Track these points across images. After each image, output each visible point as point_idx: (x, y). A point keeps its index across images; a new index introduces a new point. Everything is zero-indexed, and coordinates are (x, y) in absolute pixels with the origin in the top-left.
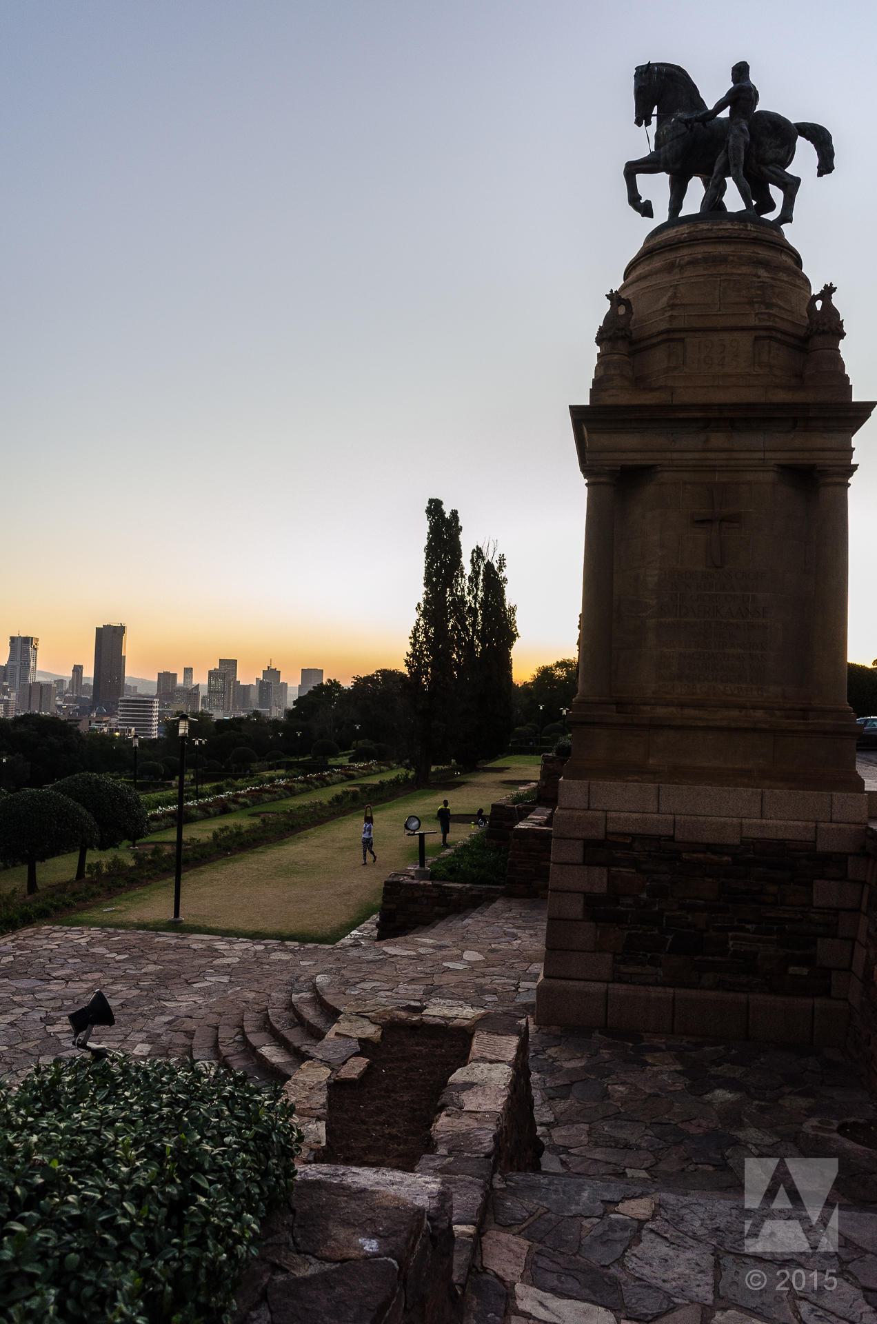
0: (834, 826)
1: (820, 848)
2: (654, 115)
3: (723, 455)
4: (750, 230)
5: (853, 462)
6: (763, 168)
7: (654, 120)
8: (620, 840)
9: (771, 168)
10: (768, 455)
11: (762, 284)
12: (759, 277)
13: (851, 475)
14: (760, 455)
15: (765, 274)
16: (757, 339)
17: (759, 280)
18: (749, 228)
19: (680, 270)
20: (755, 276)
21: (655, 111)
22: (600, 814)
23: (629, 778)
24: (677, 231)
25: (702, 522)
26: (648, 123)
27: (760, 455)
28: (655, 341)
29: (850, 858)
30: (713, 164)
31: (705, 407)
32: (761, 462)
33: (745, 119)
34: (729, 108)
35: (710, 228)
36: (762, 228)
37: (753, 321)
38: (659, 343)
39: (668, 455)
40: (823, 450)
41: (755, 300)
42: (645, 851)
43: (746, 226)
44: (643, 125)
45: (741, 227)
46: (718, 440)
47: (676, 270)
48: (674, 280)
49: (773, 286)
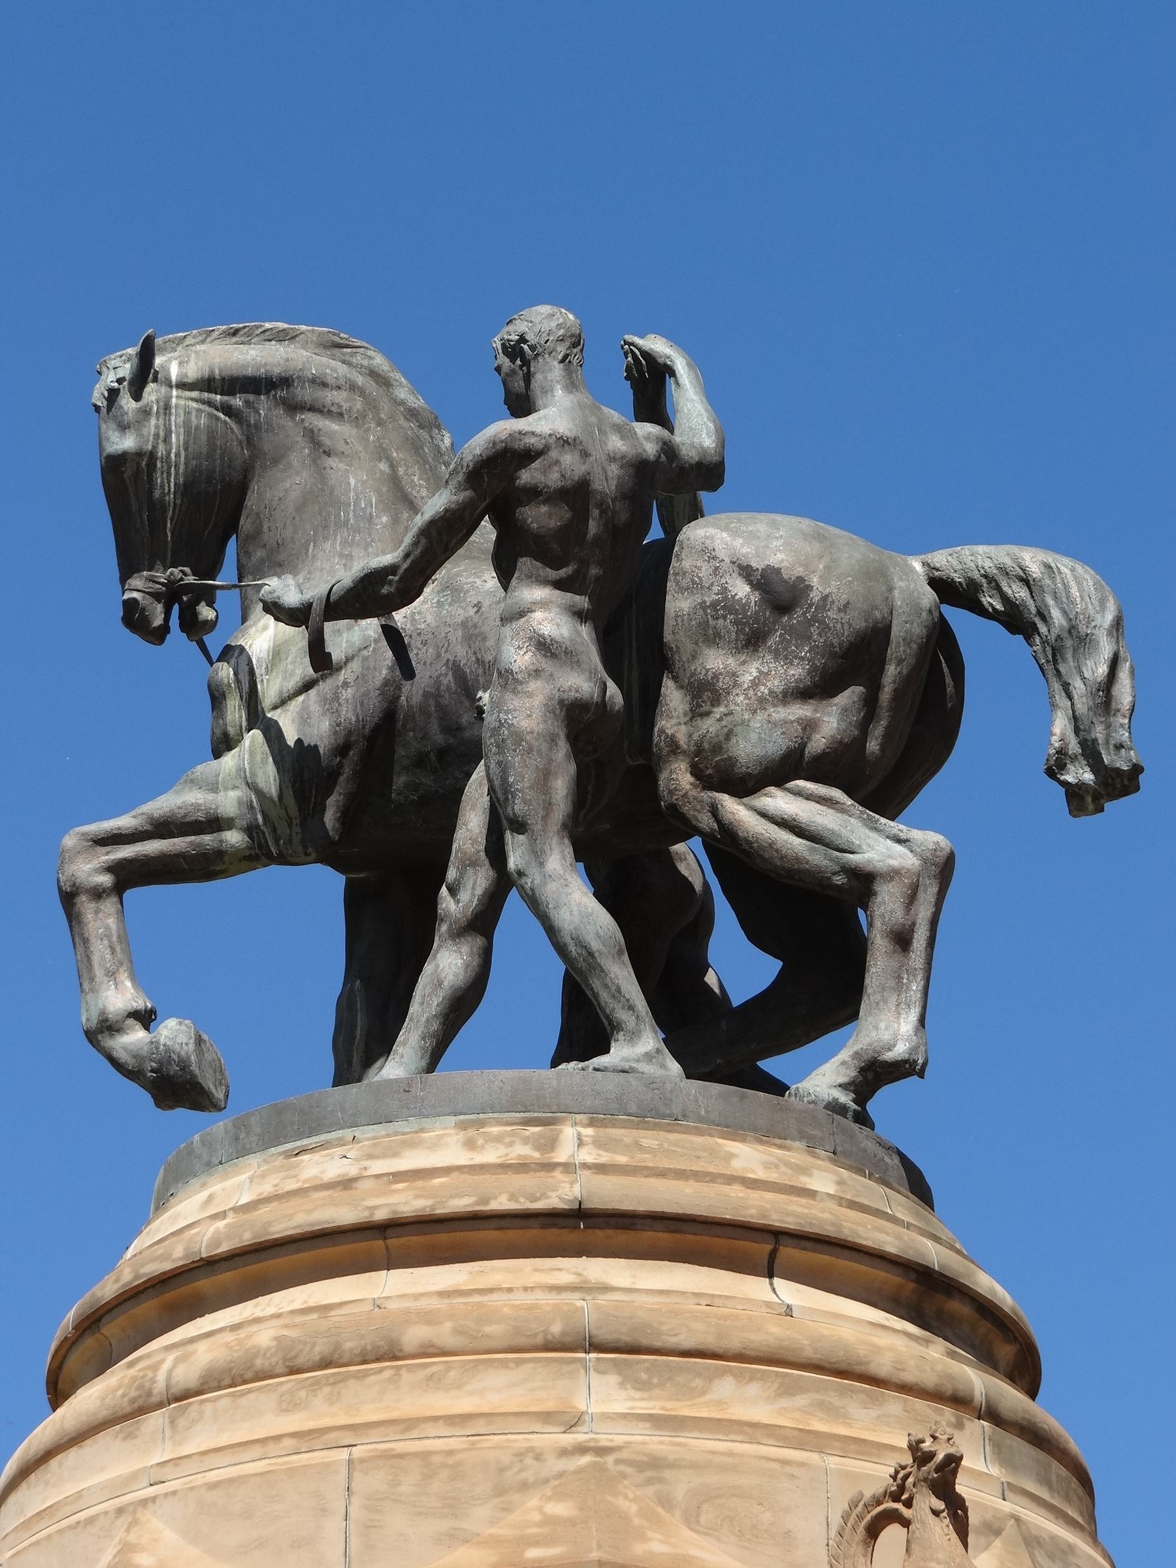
4: (568, 1167)
6: (735, 810)
9: (778, 801)
11: (586, 1460)
12: (574, 1422)
18: (561, 1156)
20: (547, 1417)
24: (210, 1199)
35: (353, 1171)
36: (649, 1139)
43: (551, 1144)
44: (176, 634)
45: (522, 1151)
48: (135, 1475)
49: (654, 1465)
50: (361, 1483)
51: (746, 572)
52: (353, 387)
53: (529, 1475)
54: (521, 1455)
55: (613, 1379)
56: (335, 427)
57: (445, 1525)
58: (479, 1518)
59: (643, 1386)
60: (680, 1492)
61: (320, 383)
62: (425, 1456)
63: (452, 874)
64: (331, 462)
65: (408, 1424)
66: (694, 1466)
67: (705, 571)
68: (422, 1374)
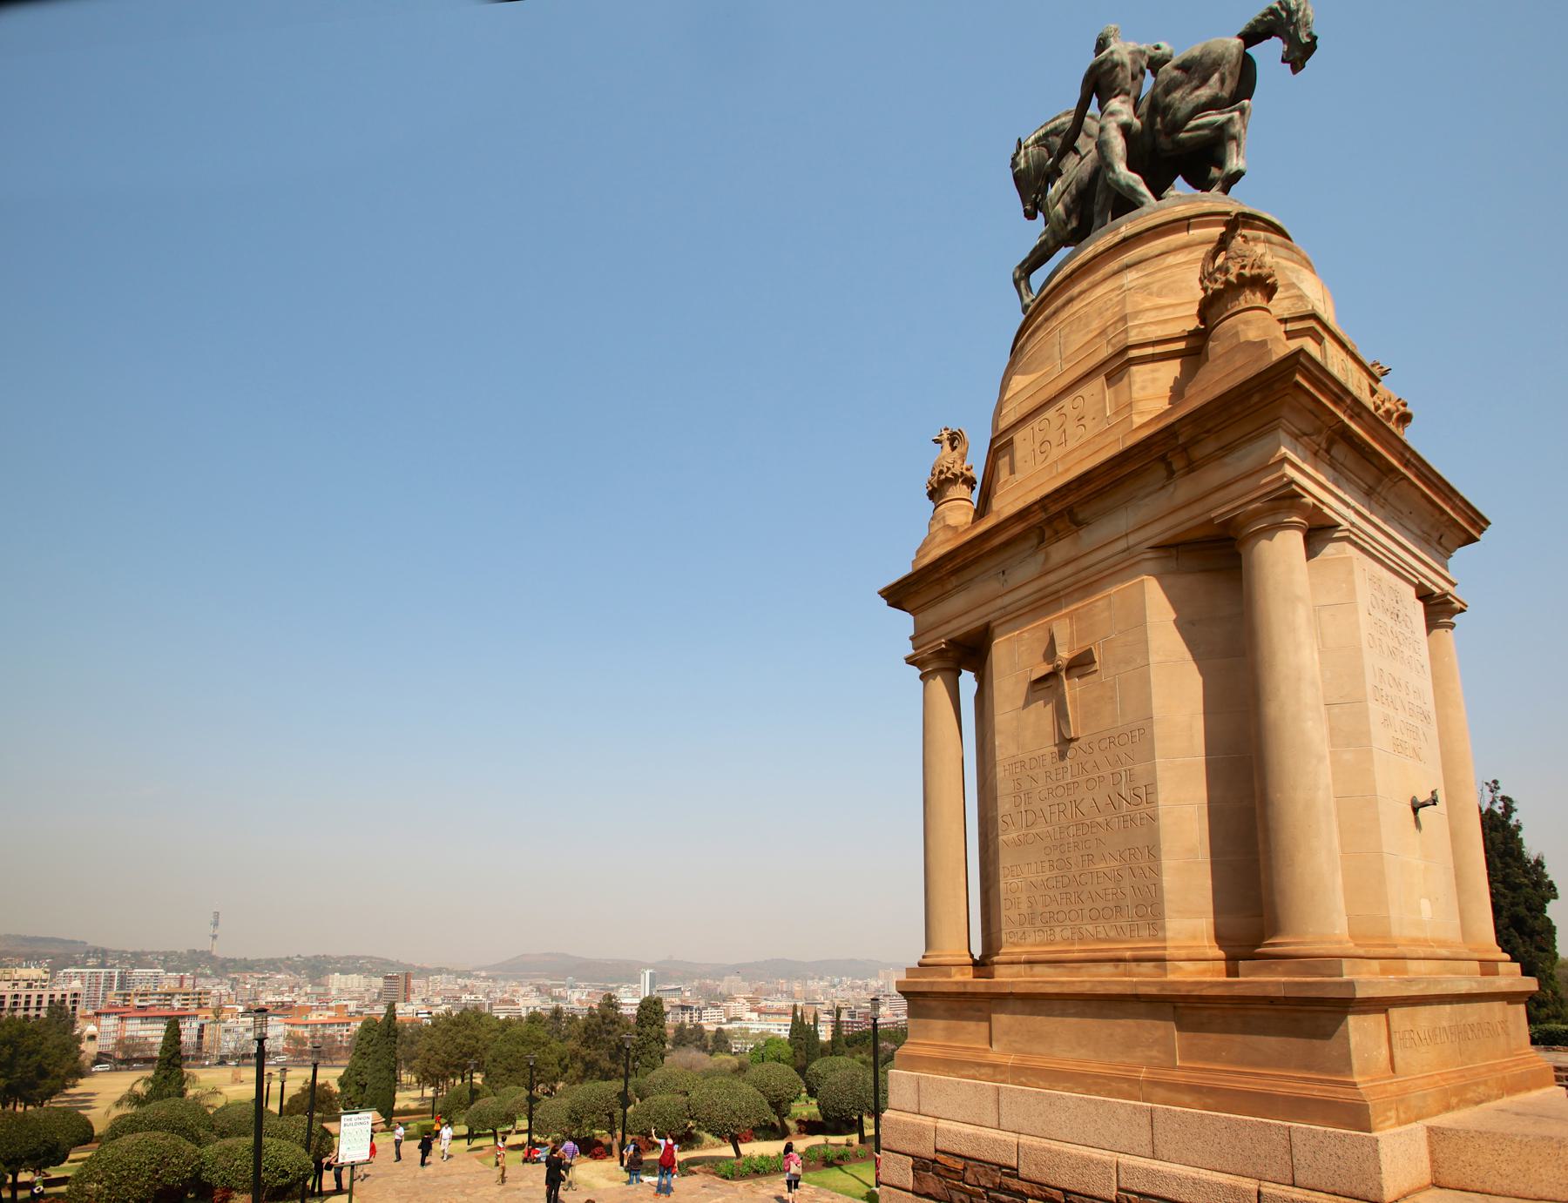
3: (1069, 569)
33: (1116, 96)
46: (1060, 550)
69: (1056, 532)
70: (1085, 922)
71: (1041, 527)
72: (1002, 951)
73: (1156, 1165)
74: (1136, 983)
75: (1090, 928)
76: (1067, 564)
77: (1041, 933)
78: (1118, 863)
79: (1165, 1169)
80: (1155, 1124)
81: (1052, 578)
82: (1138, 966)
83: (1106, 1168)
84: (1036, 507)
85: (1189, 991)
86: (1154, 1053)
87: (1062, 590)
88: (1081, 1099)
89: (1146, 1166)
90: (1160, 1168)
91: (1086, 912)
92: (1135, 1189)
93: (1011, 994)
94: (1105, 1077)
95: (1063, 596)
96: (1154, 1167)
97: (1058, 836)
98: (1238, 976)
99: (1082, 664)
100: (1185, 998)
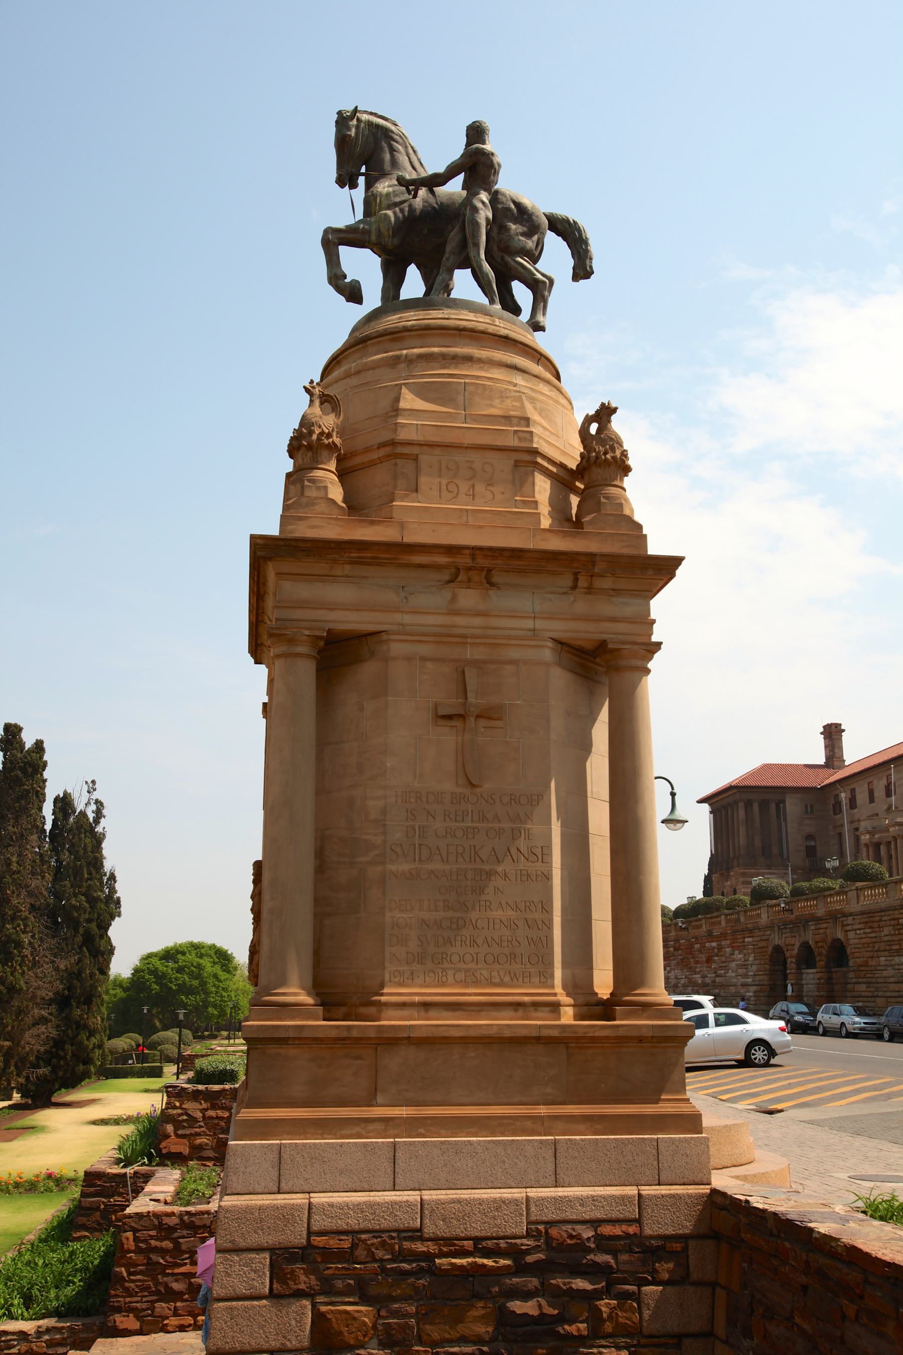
0: (664, 1190)
1: (648, 1231)
2: (362, 174)
3: (478, 621)
5: (654, 638)
6: (508, 259)
7: (361, 180)
8: (333, 1243)
10: (539, 624)
12: (515, 385)
13: (651, 659)
14: (529, 624)
15: (523, 383)
16: (517, 464)
17: (515, 388)
18: (497, 323)
19: (408, 366)
21: (363, 170)
22: (298, 1199)
23: (343, 1132)
25: (449, 717)
26: (353, 186)
27: (529, 624)
28: (374, 456)
29: (692, 1243)
30: (444, 245)
31: (451, 550)
32: (530, 633)
34: (461, 176)
36: (513, 326)
37: (514, 442)
38: (380, 460)
39: (398, 617)
40: (613, 620)
41: (512, 413)
42: (375, 1260)
43: (494, 321)
46: (469, 598)
47: (402, 366)
50: (468, 388)
51: (514, 202)
52: (401, 136)
53: (508, 395)
54: (506, 389)
55: (520, 377)
56: (395, 144)
57: (489, 402)
58: (497, 402)
59: (527, 381)
60: (538, 407)
61: (392, 132)
62: (484, 385)
63: (447, 255)
64: (395, 153)
65: (478, 377)
66: (540, 401)
67: (504, 200)
68: (478, 366)
69: (469, 580)
70: (479, 966)
71: (459, 569)
72: (385, 991)
73: (561, 1192)
74: (540, 1026)
75: (485, 973)
76: (478, 614)
77: (432, 974)
78: (514, 913)
79: (569, 1194)
80: (558, 1154)
81: (460, 620)
82: (536, 1010)
83: (517, 1206)
84: (467, 552)
85: (585, 1033)
86: (549, 1090)
87: (470, 637)
88: (489, 1142)
89: (553, 1194)
90: (566, 1194)
91: (481, 957)
92: (544, 1218)
93: (409, 1038)
94: (510, 1117)
95: (470, 643)
96: (560, 1194)
97: (454, 877)
98: (614, 1019)
99: (489, 714)
100: (578, 1039)
